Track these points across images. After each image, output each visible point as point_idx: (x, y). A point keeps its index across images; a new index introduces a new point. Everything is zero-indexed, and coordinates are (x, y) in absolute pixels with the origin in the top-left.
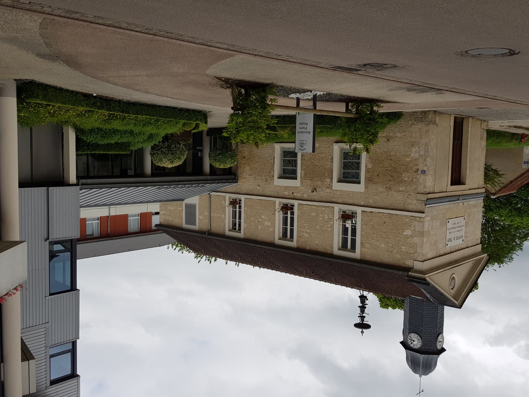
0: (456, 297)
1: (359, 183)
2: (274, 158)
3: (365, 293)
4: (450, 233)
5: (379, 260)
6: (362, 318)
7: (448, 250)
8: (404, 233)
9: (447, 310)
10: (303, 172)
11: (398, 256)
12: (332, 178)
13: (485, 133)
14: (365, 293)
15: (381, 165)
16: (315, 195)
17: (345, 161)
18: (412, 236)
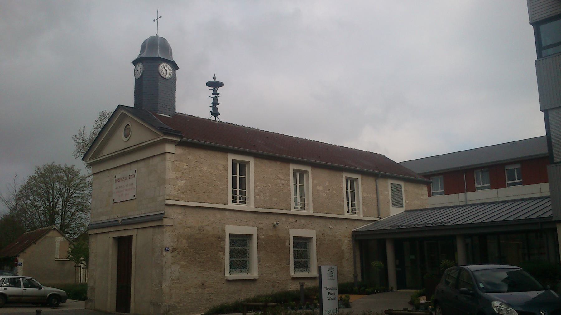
0: (124, 116)
1: (231, 235)
2: (317, 260)
3: (213, 118)
4: (132, 184)
5: (209, 152)
6: (215, 93)
7: (134, 167)
8: (184, 182)
9: (131, 103)
10: (287, 244)
11: (190, 157)
12: (258, 239)
13: (89, 296)
14: (213, 118)
15: (209, 256)
16: (274, 220)
17: (245, 259)
18: (177, 178)
